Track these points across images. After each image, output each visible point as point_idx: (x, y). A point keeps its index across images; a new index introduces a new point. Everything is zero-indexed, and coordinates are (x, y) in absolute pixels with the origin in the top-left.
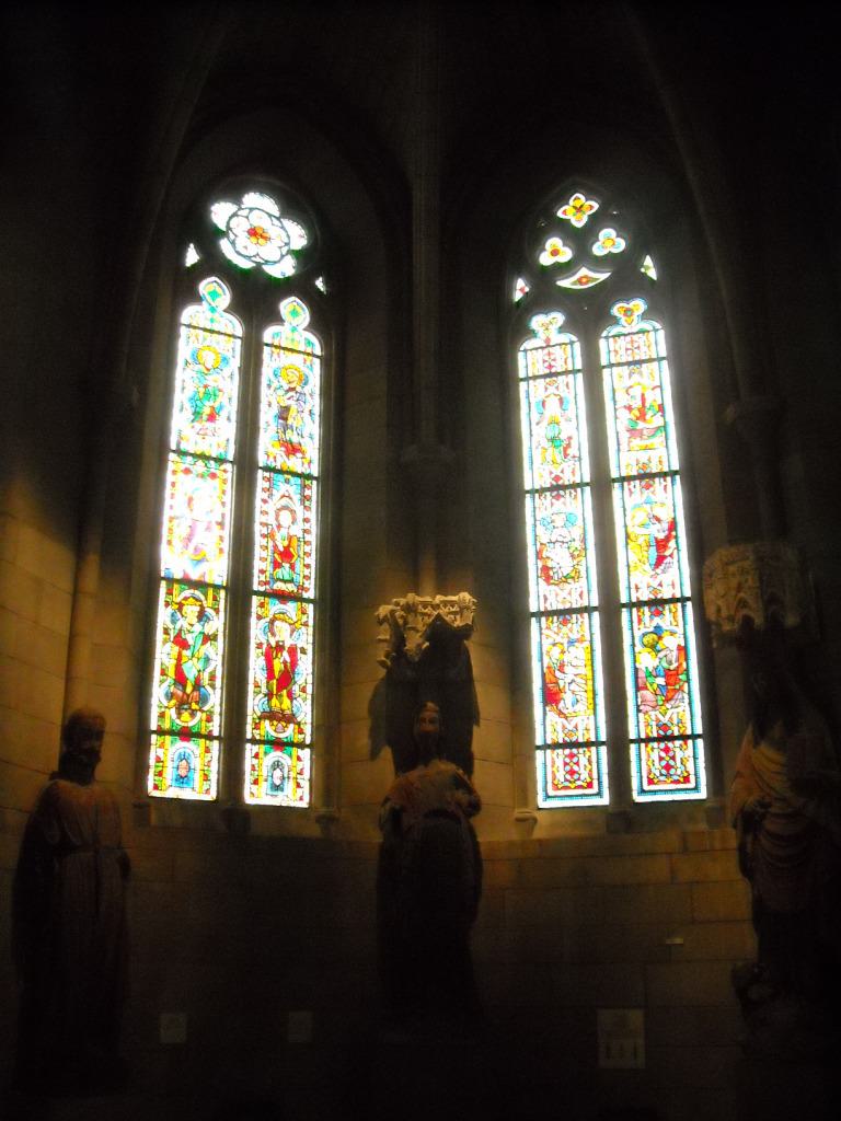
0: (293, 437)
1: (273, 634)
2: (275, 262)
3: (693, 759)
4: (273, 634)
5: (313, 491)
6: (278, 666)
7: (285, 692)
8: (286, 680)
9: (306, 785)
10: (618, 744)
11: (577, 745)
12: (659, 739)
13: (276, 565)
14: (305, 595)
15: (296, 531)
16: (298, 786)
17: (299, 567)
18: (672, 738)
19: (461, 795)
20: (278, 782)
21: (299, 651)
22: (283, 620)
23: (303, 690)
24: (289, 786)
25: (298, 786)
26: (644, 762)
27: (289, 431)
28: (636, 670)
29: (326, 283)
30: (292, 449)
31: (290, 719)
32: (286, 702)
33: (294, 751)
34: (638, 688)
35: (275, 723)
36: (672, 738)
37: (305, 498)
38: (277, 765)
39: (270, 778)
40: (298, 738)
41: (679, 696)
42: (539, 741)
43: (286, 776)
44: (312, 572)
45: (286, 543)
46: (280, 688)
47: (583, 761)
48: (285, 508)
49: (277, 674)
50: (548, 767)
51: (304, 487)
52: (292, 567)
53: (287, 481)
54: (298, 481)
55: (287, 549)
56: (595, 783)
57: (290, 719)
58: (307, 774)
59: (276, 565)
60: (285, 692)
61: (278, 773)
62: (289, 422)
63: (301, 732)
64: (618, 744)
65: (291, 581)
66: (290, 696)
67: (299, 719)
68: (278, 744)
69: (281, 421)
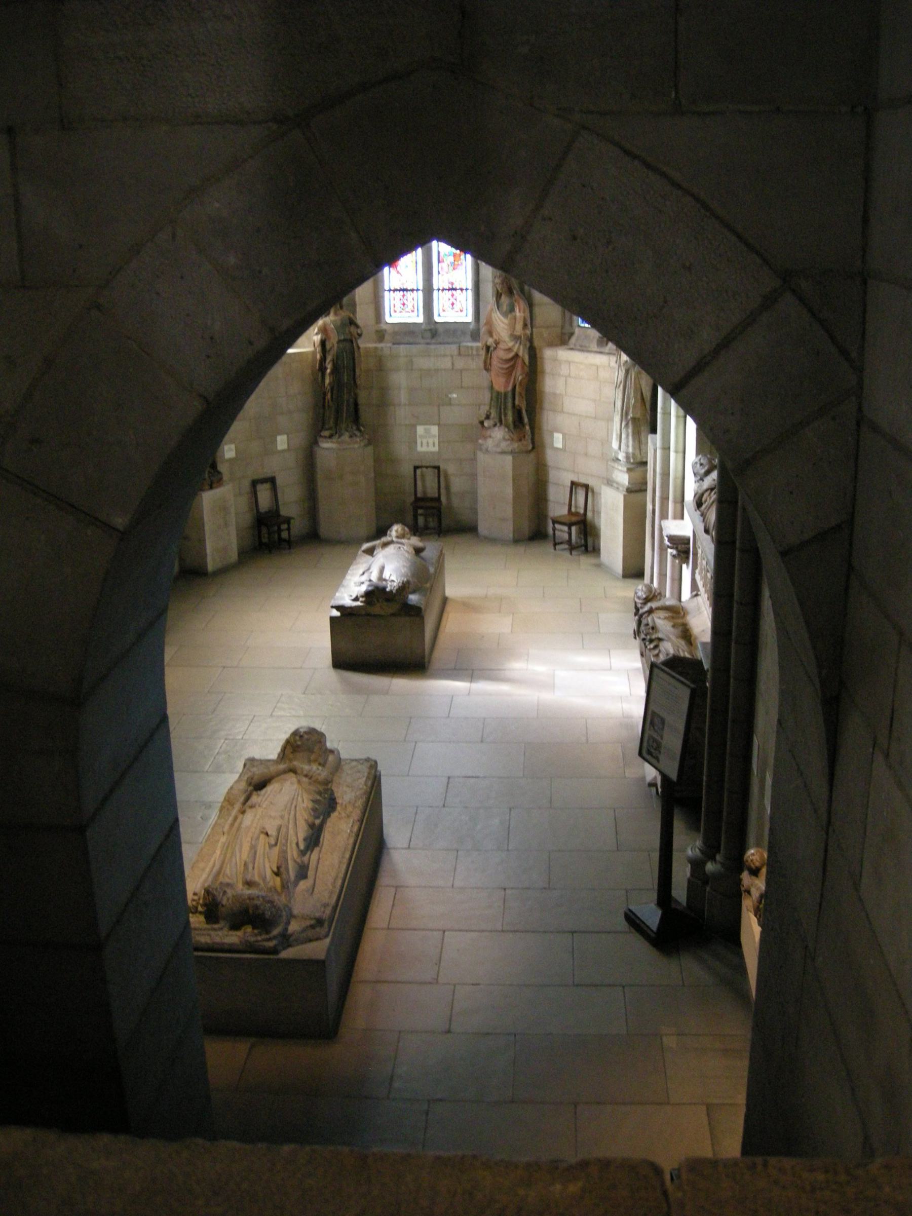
3: (466, 301)
10: (428, 291)
11: (407, 290)
12: (449, 290)
18: (455, 289)
19: (352, 329)
26: (441, 301)
28: (439, 253)
34: (439, 262)
36: (455, 289)
41: (460, 267)
42: (387, 288)
47: (410, 299)
50: (390, 301)
56: (416, 310)
64: (428, 291)
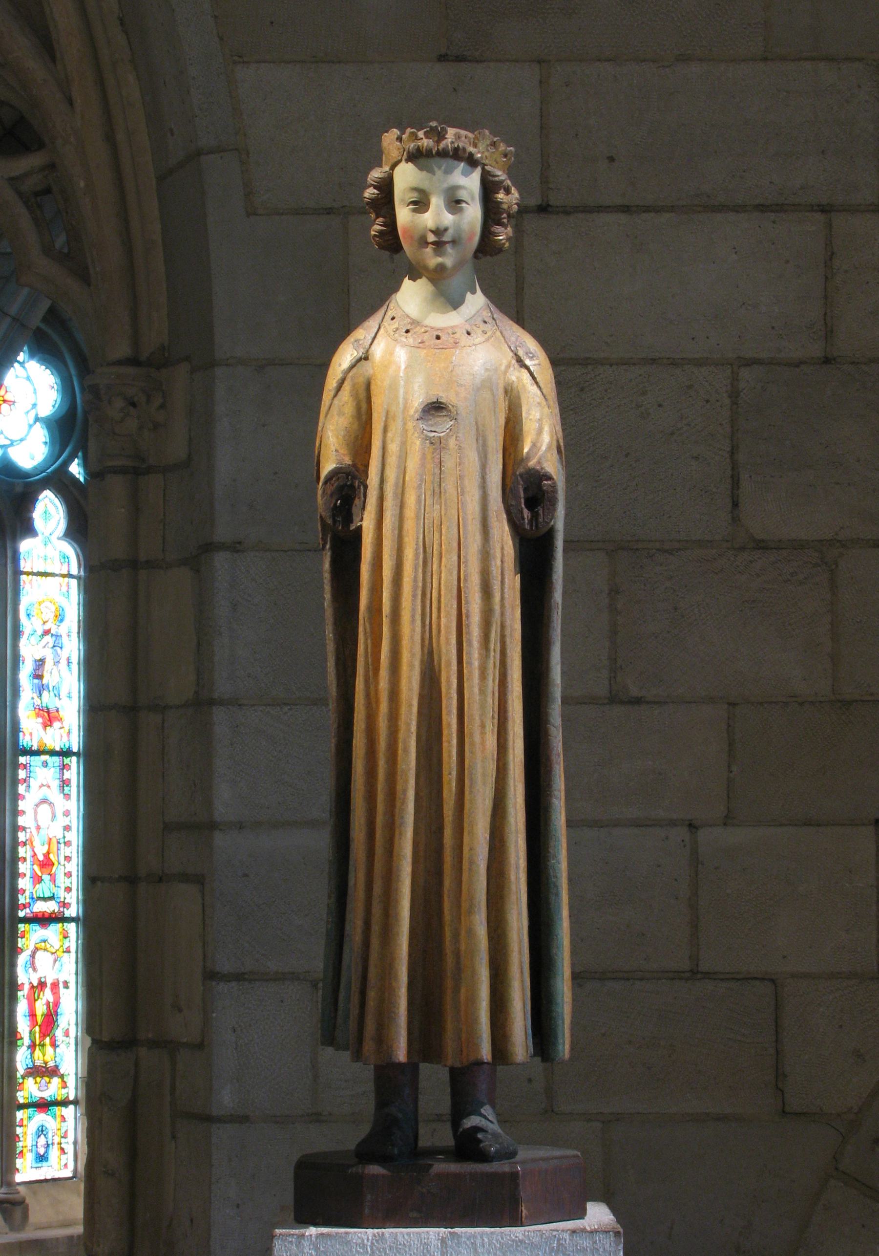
0: (48, 699)
1: (35, 969)
2: (22, 440)
4: (35, 969)
5: (75, 771)
6: (41, 1009)
7: (47, 1040)
8: (50, 1021)
9: (70, 1149)
13: (37, 880)
14: (68, 913)
15: (56, 831)
16: (63, 1151)
17: (61, 880)
20: (42, 1151)
21: (61, 985)
22: (45, 950)
23: (67, 1034)
24: (54, 1152)
25: (63, 1151)
27: (45, 694)
29: (86, 465)
30: (49, 717)
31: (52, 1072)
32: (49, 1049)
33: (56, 1110)
35: (38, 1079)
37: (65, 783)
38: (41, 1131)
39: (34, 1147)
40: (61, 1095)
43: (50, 1142)
44: (75, 882)
45: (45, 849)
46: (43, 1035)
48: (44, 801)
49: (40, 1019)
51: (64, 767)
52: (53, 880)
53: (45, 764)
54: (56, 760)
55: (47, 855)
57: (52, 1072)
58: (71, 1137)
59: (37, 880)
60: (47, 1040)
61: (42, 1141)
62: (45, 681)
63: (64, 1085)
65: (52, 898)
66: (54, 1045)
67: (62, 1071)
68: (43, 1105)
69: (36, 681)
